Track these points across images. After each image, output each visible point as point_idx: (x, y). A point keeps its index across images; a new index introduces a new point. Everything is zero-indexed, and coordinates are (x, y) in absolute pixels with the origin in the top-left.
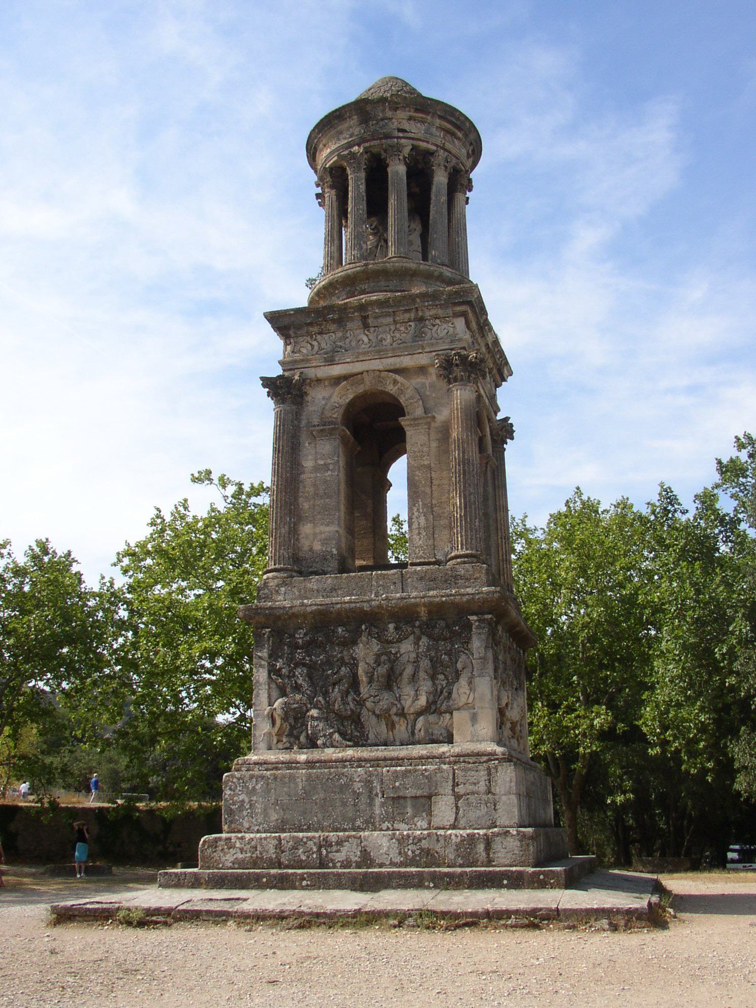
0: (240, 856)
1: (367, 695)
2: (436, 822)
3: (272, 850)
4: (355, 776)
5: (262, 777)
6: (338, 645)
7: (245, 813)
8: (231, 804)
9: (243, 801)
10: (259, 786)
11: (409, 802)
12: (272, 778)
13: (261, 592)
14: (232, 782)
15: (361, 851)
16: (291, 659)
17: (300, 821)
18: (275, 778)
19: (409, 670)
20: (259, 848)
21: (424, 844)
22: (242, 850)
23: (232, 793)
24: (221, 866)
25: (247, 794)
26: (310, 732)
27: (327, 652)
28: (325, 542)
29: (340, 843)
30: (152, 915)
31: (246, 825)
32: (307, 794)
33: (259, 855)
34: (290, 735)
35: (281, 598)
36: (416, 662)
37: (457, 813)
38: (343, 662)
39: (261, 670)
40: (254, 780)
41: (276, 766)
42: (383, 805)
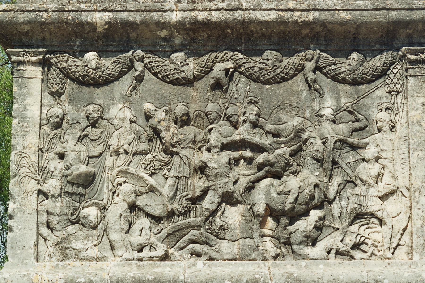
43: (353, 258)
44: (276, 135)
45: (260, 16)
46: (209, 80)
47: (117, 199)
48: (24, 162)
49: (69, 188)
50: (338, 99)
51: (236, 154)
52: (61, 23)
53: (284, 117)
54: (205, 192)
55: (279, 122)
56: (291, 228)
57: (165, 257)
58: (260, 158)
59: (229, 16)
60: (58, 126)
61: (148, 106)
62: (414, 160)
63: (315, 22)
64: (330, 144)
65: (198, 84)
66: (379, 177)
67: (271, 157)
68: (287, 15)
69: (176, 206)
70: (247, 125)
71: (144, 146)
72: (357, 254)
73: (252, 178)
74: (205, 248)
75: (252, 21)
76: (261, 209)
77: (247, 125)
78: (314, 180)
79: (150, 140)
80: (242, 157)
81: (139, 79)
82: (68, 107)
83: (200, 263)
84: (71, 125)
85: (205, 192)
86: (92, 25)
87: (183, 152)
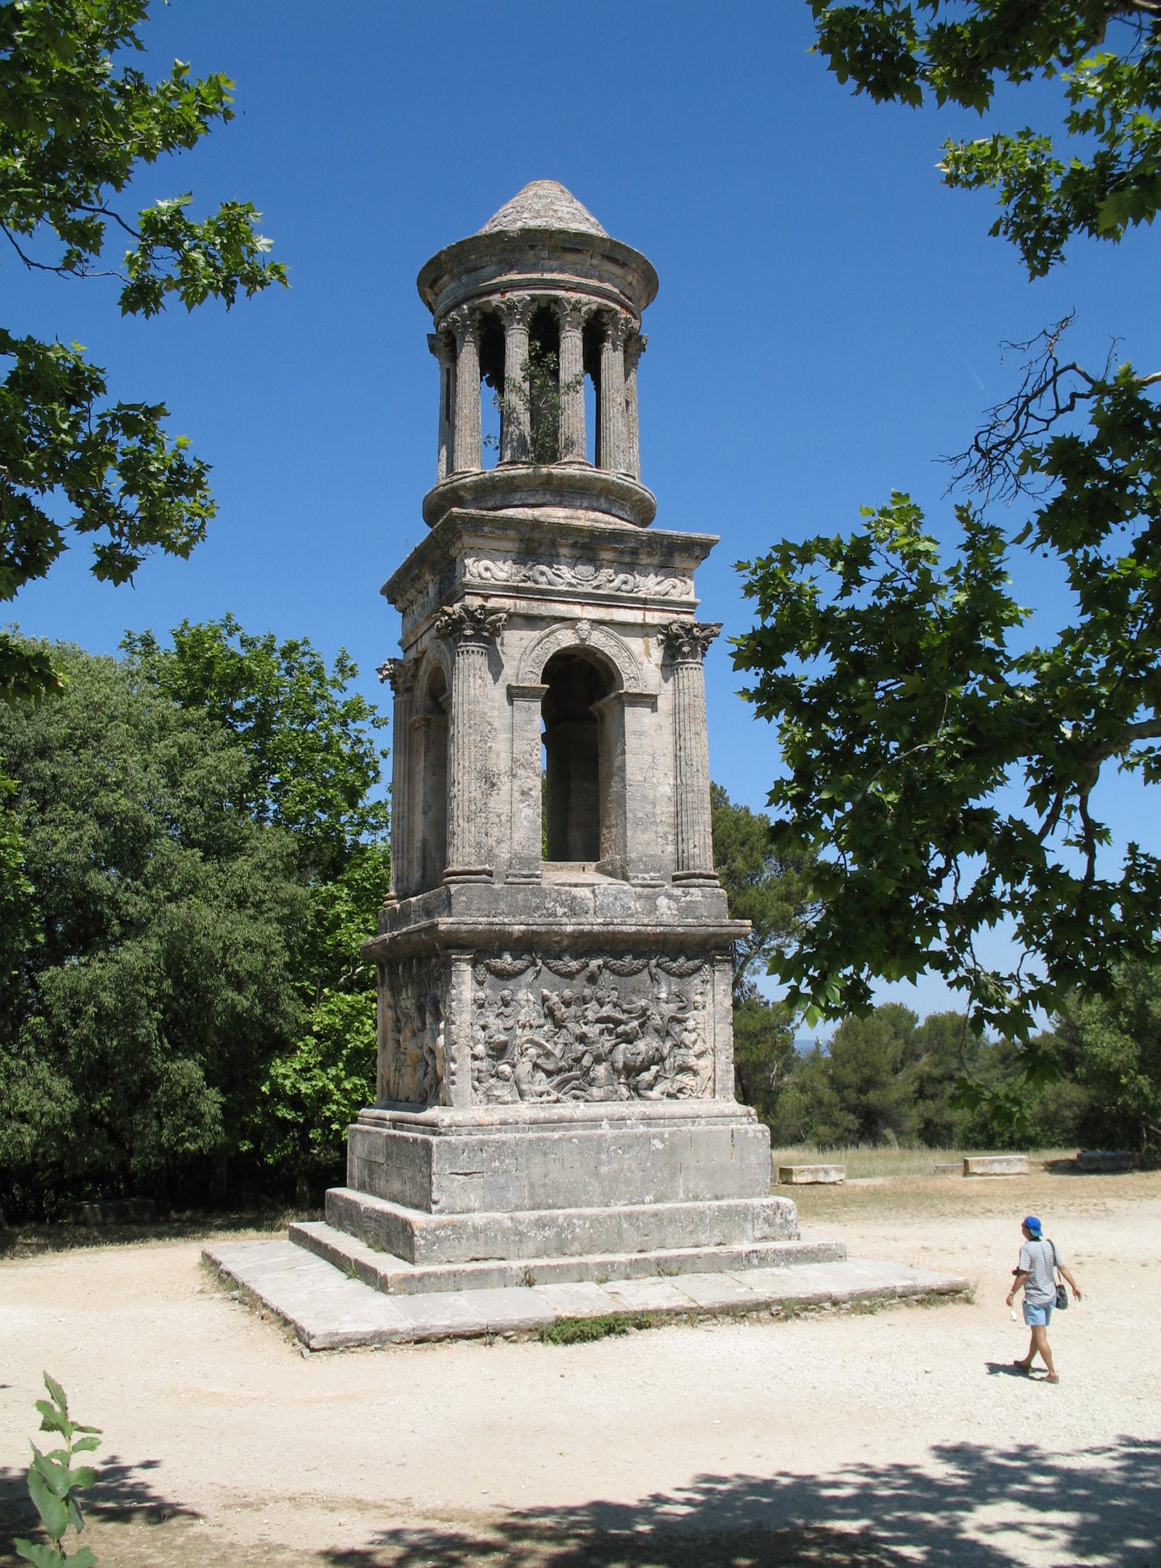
43: (677, 1098)
44: (630, 1012)
45: (624, 928)
46: (586, 973)
47: (524, 1059)
48: (462, 1034)
49: (490, 1052)
50: (669, 986)
51: (603, 1026)
52: (490, 931)
53: (634, 999)
54: (584, 1054)
55: (632, 1002)
56: (638, 1078)
57: (557, 1101)
58: (621, 1029)
59: (605, 928)
60: (481, 1006)
61: (546, 992)
62: (717, 1031)
63: (661, 933)
64: (666, 1019)
65: (577, 977)
66: (694, 1043)
67: (627, 1028)
68: (643, 928)
69: (562, 1063)
70: (610, 1005)
71: (542, 1021)
72: (681, 1096)
73: (613, 1042)
74: (583, 1093)
75: (619, 932)
76: (620, 1065)
77: (610, 1005)
78: (655, 1045)
79: (546, 1017)
80: (607, 1028)
81: (539, 972)
82: (488, 992)
83: (582, 1104)
84: (490, 1005)
85: (584, 1054)
86: (511, 934)
87: (569, 1025)
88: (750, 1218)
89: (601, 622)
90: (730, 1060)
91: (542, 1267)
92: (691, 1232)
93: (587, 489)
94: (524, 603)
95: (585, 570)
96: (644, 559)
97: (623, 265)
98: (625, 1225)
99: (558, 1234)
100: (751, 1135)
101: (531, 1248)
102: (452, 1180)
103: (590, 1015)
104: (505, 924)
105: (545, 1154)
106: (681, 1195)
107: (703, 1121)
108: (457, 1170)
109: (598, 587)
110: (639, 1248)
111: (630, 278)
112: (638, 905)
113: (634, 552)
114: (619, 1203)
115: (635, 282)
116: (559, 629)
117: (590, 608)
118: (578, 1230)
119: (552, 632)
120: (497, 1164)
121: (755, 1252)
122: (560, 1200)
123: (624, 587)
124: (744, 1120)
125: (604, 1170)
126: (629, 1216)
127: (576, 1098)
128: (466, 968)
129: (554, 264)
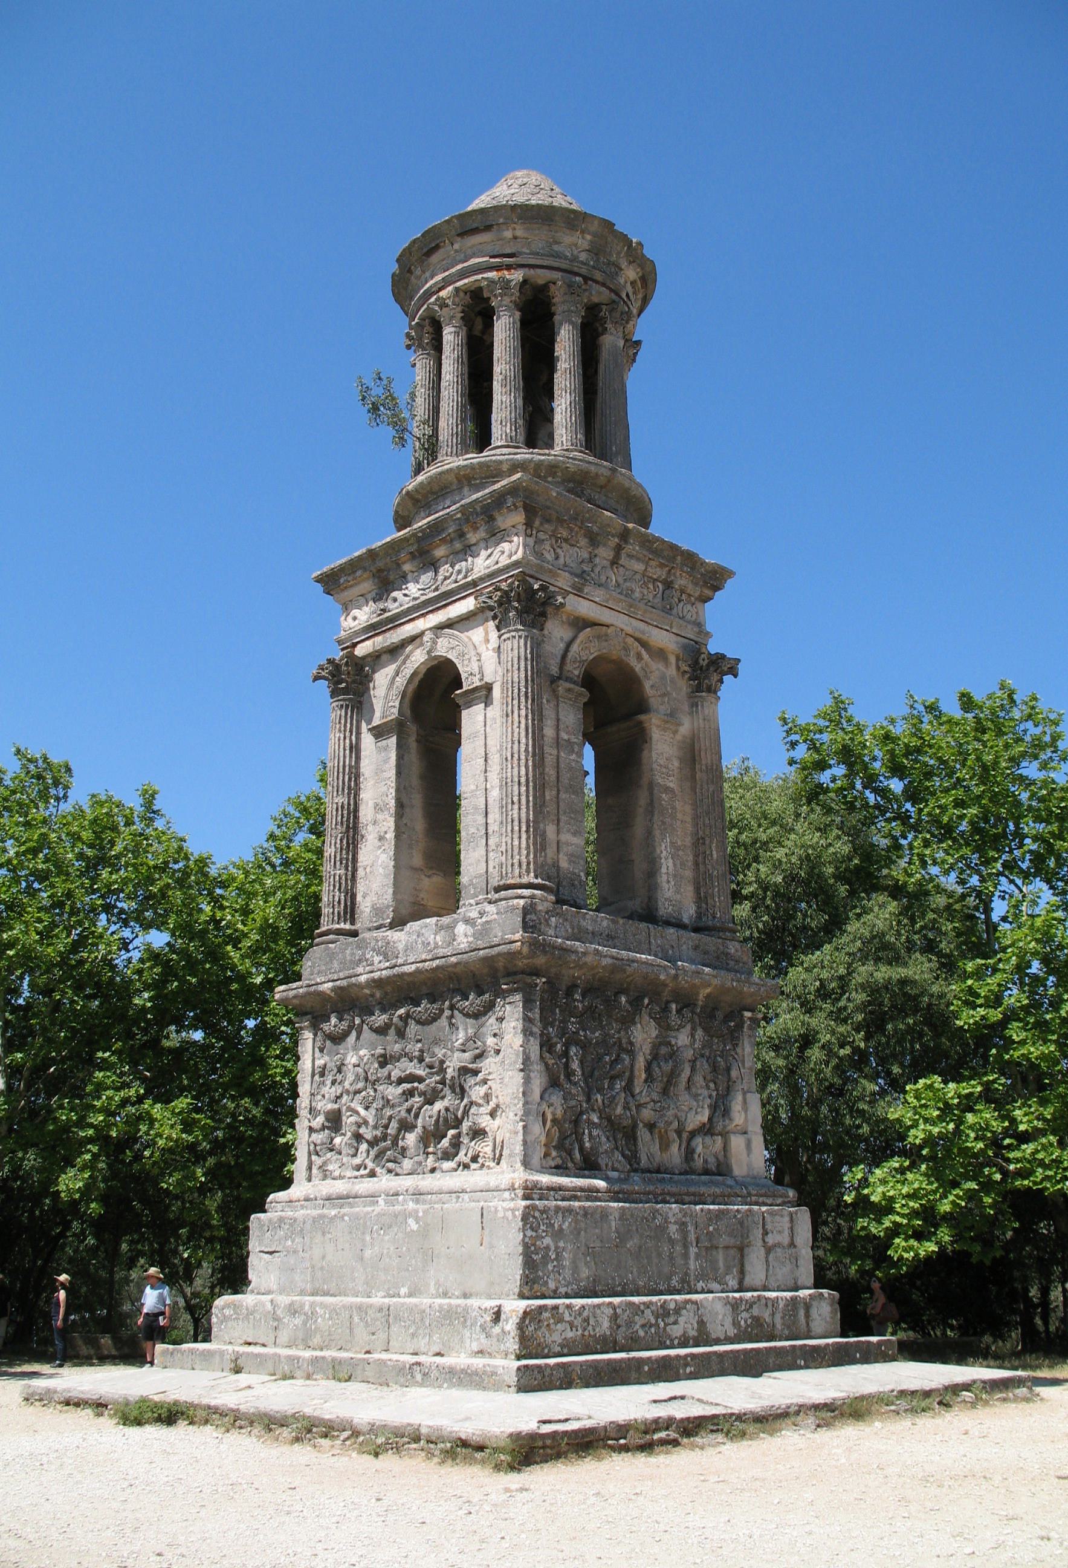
0: (570, 1334)
1: (648, 1099)
2: (748, 1281)
3: (606, 1324)
4: (670, 1215)
5: (569, 1210)
6: (616, 1020)
7: (550, 1267)
8: (532, 1252)
9: (548, 1248)
10: (567, 1224)
11: (721, 1251)
12: (582, 1212)
13: (529, 917)
14: (534, 1217)
15: (698, 1323)
16: (563, 1031)
17: (613, 1279)
18: (586, 1214)
19: (687, 1072)
20: (592, 1322)
21: (755, 1311)
22: (572, 1326)
23: (534, 1234)
24: (546, 1351)
25: (552, 1236)
26: (587, 1145)
27: (602, 1028)
28: (572, 858)
29: (678, 1311)
30: (655, 1431)
31: (552, 1285)
32: (623, 1237)
33: (592, 1333)
34: (560, 1147)
35: (551, 932)
36: (693, 1062)
37: (767, 1270)
38: (622, 1049)
39: (532, 1039)
40: (560, 1214)
41: (573, 1194)
42: (698, 1256)
57: (372, 1174)
63: (438, 967)
72: (473, 1166)
88: (468, 1323)
89: (441, 627)
90: (518, 1118)
91: (248, 1354)
92: (413, 1335)
93: (446, 488)
94: (379, 639)
95: (426, 578)
96: (472, 538)
97: (488, 228)
98: (356, 1319)
99: (305, 1323)
100: (500, 1214)
101: (284, 1336)
102: (261, 1258)
103: (396, 1074)
104: (317, 984)
105: (324, 1234)
106: (433, 1290)
107: (466, 1196)
108: (263, 1249)
109: (436, 589)
110: (367, 1348)
111: (508, 234)
112: (438, 938)
113: (462, 535)
114: (379, 1294)
115: (519, 233)
116: (412, 652)
117: (431, 616)
118: (319, 1320)
119: (408, 656)
120: (289, 1243)
121: (418, 1364)
122: (332, 1287)
123: (460, 577)
124: (507, 1194)
125: (368, 1253)
126: (360, 1308)
127: (390, 1171)
128: (308, 1035)
129: (428, 274)
